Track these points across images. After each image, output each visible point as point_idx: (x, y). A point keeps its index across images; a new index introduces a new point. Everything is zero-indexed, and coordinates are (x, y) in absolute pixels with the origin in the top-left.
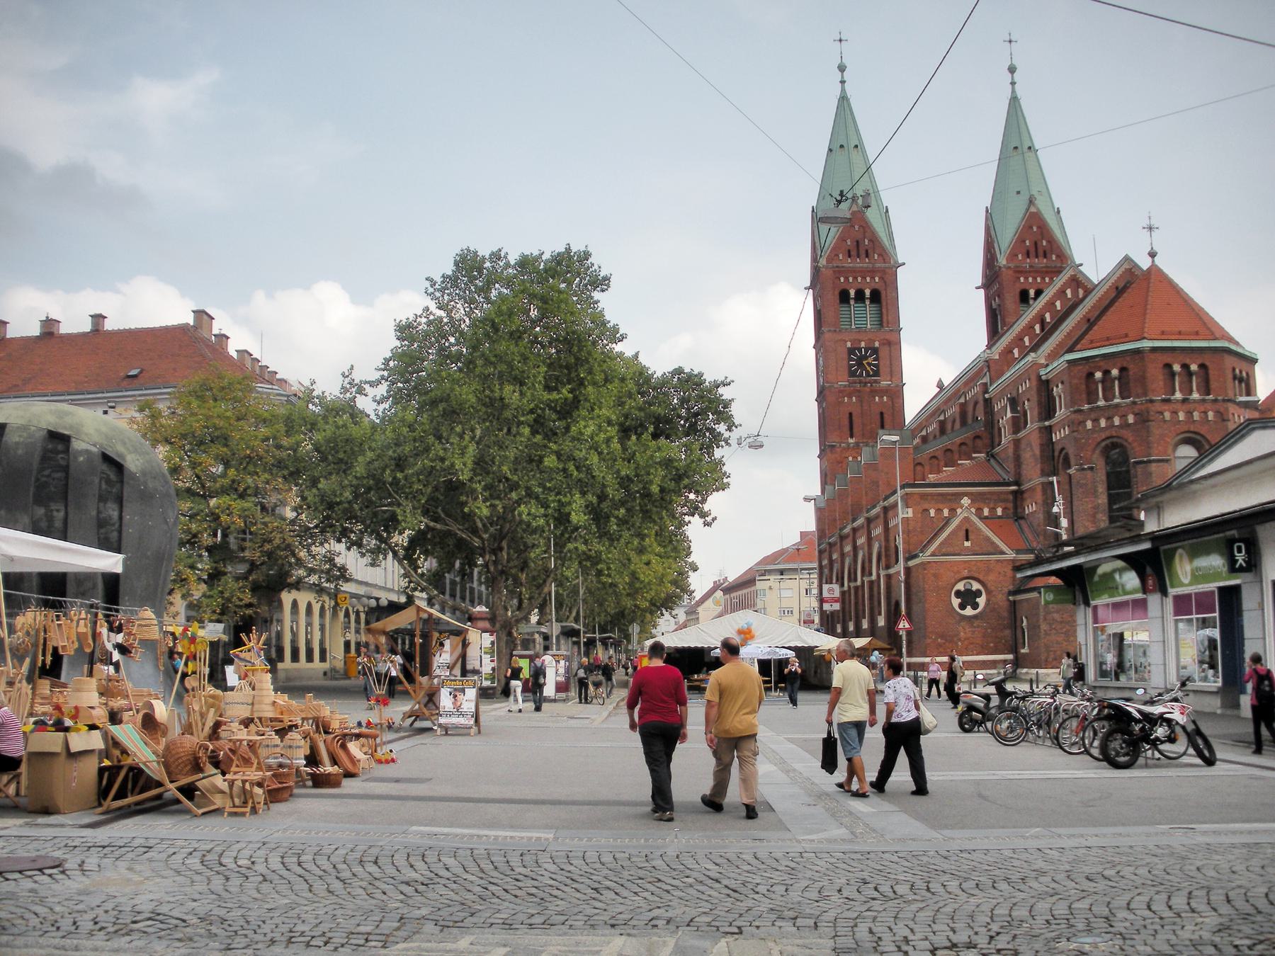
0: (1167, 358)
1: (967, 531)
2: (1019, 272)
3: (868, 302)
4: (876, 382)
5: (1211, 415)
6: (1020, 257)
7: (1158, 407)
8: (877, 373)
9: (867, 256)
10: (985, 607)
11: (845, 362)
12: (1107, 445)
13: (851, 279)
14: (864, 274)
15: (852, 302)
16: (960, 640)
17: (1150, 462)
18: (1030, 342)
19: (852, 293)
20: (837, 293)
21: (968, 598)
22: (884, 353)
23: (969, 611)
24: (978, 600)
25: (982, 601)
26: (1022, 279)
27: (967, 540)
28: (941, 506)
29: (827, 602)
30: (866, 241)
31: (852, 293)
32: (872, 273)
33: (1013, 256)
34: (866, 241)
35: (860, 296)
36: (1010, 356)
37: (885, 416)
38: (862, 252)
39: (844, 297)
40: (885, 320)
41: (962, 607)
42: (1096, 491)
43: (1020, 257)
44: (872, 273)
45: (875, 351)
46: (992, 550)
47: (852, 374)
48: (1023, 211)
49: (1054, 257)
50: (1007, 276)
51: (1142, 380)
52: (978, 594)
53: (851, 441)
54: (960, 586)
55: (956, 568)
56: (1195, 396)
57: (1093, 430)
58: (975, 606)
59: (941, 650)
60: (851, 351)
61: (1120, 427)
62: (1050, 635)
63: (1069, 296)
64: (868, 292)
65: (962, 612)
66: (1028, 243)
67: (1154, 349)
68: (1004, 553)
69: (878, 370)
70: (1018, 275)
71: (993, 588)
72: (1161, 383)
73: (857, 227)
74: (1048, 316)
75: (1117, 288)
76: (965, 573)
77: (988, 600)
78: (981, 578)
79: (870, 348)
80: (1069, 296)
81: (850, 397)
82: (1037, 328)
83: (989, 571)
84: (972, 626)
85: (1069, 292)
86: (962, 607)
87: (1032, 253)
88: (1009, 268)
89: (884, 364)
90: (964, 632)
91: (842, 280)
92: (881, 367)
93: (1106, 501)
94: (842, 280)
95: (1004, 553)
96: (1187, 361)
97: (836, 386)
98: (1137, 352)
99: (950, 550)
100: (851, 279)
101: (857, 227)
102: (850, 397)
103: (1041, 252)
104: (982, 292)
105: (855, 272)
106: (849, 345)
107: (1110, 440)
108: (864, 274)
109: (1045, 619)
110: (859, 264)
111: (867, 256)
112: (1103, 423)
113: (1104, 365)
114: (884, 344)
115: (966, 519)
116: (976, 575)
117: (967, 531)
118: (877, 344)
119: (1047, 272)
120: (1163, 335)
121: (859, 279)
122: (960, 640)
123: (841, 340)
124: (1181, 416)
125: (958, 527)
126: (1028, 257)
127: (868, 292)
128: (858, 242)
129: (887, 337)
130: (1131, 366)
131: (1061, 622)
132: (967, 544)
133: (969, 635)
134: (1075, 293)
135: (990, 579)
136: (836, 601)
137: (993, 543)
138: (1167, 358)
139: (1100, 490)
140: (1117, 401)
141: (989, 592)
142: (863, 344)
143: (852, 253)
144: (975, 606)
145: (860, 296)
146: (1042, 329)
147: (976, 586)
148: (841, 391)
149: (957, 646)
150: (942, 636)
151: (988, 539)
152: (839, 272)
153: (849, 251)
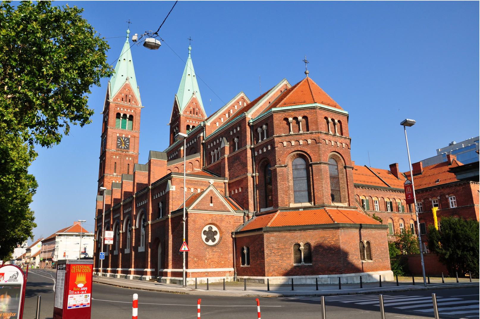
0: (326, 114)
1: (211, 197)
2: (187, 118)
3: (127, 119)
4: (127, 151)
5: (344, 144)
6: (188, 113)
7: (323, 136)
8: (128, 148)
9: (129, 102)
10: (219, 242)
11: (116, 142)
12: (294, 155)
13: (122, 109)
14: (127, 108)
15: (121, 118)
16: (206, 259)
17: (320, 163)
18: (219, 125)
19: (122, 115)
20: (115, 114)
21: (210, 235)
22: (132, 140)
23: (210, 243)
24: (215, 237)
25: (217, 237)
26: (188, 121)
27: (211, 203)
28: (190, 186)
29: (107, 240)
30: (130, 96)
31: (122, 115)
32: (131, 108)
33: (185, 112)
34: (130, 96)
35: (125, 115)
36: (214, 125)
37: (130, 166)
38: (128, 100)
39: (118, 116)
40: (133, 128)
41: (207, 240)
42: (288, 179)
43: (188, 113)
44: (131, 108)
45: (128, 139)
46: (223, 209)
47: (118, 147)
48: (191, 97)
49: (200, 115)
50: (182, 119)
51: (316, 123)
52: (215, 233)
53: (115, 174)
54: (206, 228)
55: (205, 218)
56: (338, 134)
57: (287, 147)
58: (214, 240)
59: (196, 265)
60: (118, 138)
61: (303, 145)
62: (270, 256)
63: (241, 104)
64: (128, 116)
65: (207, 243)
66: (191, 108)
67: (321, 108)
68: (230, 211)
69: (129, 147)
70: (186, 119)
71: (224, 230)
72: (324, 125)
73: (127, 90)
74: (231, 111)
75: (281, 91)
76: (210, 221)
77: (221, 238)
78: (218, 224)
79: (126, 138)
80: (241, 104)
81: (116, 156)
82: (227, 115)
83: (222, 220)
84: (213, 251)
85: (240, 103)
86: (207, 240)
87: (192, 112)
88: (184, 116)
89: (131, 144)
90: (209, 254)
91: (118, 109)
92: (130, 146)
93: (292, 184)
94: (118, 109)
95: (230, 211)
96: (334, 118)
97: (111, 151)
98: (314, 108)
99: (202, 207)
100: (122, 109)
101: (127, 90)
102: (116, 156)
103: (195, 113)
104: (169, 126)
105: (124, 107)
106: (118, 135)
107: (296, 152)
108: (127, 108)
109: (267, 247)
110: (126, 104)
111: (129, 102)
112: (293, 143)
113: (295, 114)
114: (132, 137)
115: (211, 191)
116: (215, 222)
117: (211, 197)
118: (129, 137)
119: (197, 120)
120: (322, 103)
121: (125, 110)
122: (206, 259)
123: (115, 132)
124: (333, 143)
125: (207, 195)
126: (191, 113)
127: (128, 116)
128: (126, 95)
129: (134, 134)
130: (309, 116)
131: (278, 249)
132: (211, 205)
133: (211, 257)
134: (243, 103)
135: (223, 225)
136: (111, 240)
137: (224, 205)
138: (326, 114)
139: (290, 178)
140: (301, 132)
141: (221, 233)
142: (124, 136)
143: (124, 99)
144: (214, 240)
145: (125, 115)
146: (229, 117)
147: (214, 229)
148: (112, 153)
149: (205, 262)
150: (196, 257)
151: (222, 203)
152: (117, 105)
153: (123, 98)
